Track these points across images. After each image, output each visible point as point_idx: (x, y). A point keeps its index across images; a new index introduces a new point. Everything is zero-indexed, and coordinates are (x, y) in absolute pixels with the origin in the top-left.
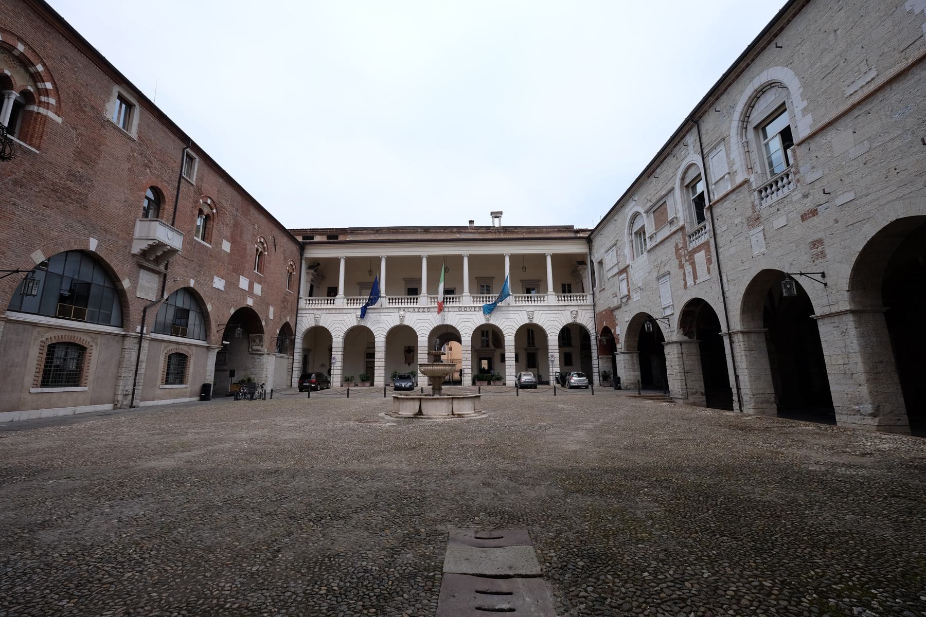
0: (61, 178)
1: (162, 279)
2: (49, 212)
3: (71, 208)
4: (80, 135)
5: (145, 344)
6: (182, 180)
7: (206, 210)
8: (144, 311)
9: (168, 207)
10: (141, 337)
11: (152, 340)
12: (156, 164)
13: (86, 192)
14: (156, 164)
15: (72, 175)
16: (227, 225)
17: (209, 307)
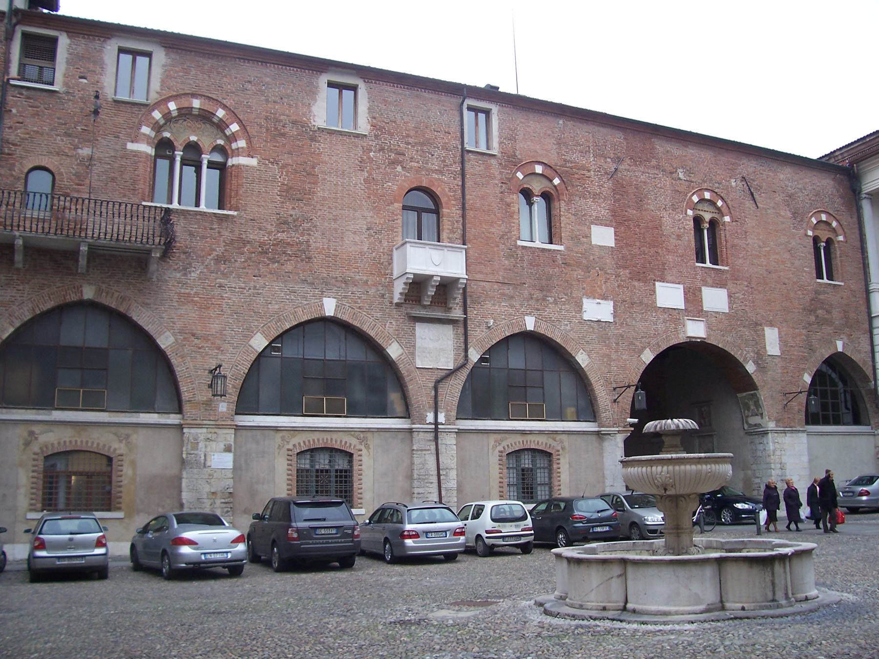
0: (270, 233)
1: (461, 330)
2: (261, 281)
3: (289, 267)
4: (285, 166)
5: (448, 441)
6: (467, 157)
7: (537, 187)
8: (436, 388)
9: (451, 211)
10: (436, 428)
11: (460, 432)
12: (412, 152)
13: (305, 238)
14: (412, 152)
15: (283, 223)
16: (595, 196)
17: (582, 359)
